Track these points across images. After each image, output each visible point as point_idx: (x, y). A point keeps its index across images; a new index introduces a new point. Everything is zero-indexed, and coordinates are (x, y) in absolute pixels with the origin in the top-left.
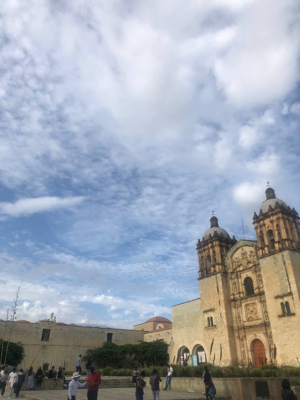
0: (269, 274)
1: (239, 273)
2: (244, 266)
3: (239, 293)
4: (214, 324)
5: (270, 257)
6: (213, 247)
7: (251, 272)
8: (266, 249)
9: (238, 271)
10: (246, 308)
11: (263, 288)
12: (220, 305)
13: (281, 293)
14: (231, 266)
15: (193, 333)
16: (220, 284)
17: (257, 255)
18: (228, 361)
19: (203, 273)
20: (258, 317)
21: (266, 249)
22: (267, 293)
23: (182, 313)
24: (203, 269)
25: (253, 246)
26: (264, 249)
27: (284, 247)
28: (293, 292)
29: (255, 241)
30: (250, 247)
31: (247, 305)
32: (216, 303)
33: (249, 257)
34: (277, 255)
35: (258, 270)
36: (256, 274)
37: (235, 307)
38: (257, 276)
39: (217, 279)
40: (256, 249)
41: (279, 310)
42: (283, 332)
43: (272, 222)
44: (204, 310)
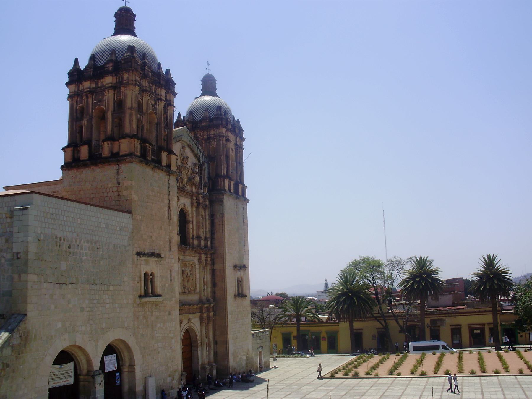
4: (159, 290)
12: (170, 250)
13: (238, 263)
18: (177, 373)
23: (75, 234)
39: (169, 187)
44: (138, 250)
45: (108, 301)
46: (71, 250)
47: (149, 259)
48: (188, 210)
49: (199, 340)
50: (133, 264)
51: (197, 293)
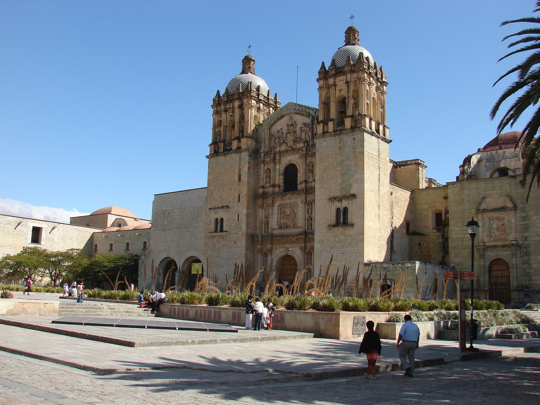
0: (327, 164)
1: (277, 155)
2: (289, 145)
3: (274, 186)
4: (225, 229)
5: (334, 137)
6: (241, 107)
7: (297, 156)
8: (331, 124)
9: (277, 152)
11: (313, 183)
12: (239, 201)
14: (267, 143)
15: (188, 239)
16: (245, 169)
17: (313, 132)
19: (218, 148)
21: (331, 126)
22: (318, 192)
24: (218, 141)
25: (309, 117)
26: (327, 124)
27: (358, 126)
28: (356, 194)
29: (312, 109)
30: (303, 117)
31: (281, 207)
32: (232, 198)
33: (298, 132)
34: (345, 136)
35: (310, 155)
36: (306, 162)
37: (263, 206)
38: (306, 165)
40: (313, 121)
41: (332, 218)
42: (331, 248)
43: (347, 83)
44: (211, 207)
45: (188, 236)
46: (170, 215)
47: (216, 210)
49: (300, 265)
50: (206, 215)
51: (297, 227)
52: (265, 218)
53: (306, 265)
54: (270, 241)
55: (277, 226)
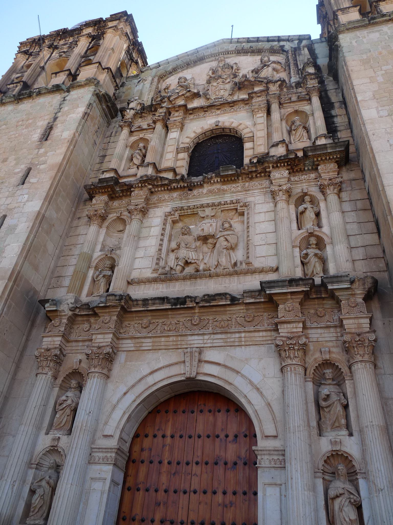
2: (213, 97)
10: (168, 227)
20: (248, 264)
37: (103, 218)
48: (234, 125)
49: (270, 429)
52: (100, 251)
53: (315, 432)
54: (115, 318)
55: (155, 270)
